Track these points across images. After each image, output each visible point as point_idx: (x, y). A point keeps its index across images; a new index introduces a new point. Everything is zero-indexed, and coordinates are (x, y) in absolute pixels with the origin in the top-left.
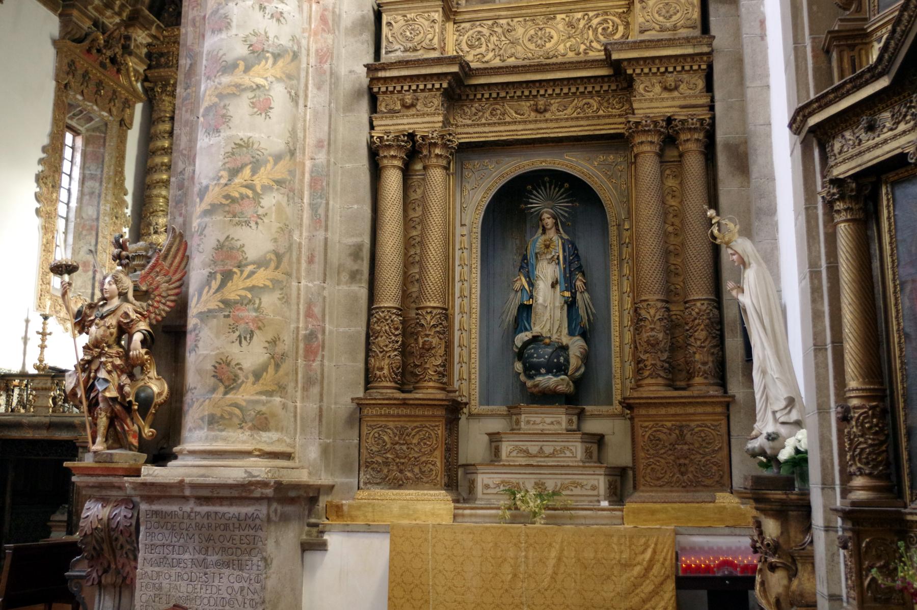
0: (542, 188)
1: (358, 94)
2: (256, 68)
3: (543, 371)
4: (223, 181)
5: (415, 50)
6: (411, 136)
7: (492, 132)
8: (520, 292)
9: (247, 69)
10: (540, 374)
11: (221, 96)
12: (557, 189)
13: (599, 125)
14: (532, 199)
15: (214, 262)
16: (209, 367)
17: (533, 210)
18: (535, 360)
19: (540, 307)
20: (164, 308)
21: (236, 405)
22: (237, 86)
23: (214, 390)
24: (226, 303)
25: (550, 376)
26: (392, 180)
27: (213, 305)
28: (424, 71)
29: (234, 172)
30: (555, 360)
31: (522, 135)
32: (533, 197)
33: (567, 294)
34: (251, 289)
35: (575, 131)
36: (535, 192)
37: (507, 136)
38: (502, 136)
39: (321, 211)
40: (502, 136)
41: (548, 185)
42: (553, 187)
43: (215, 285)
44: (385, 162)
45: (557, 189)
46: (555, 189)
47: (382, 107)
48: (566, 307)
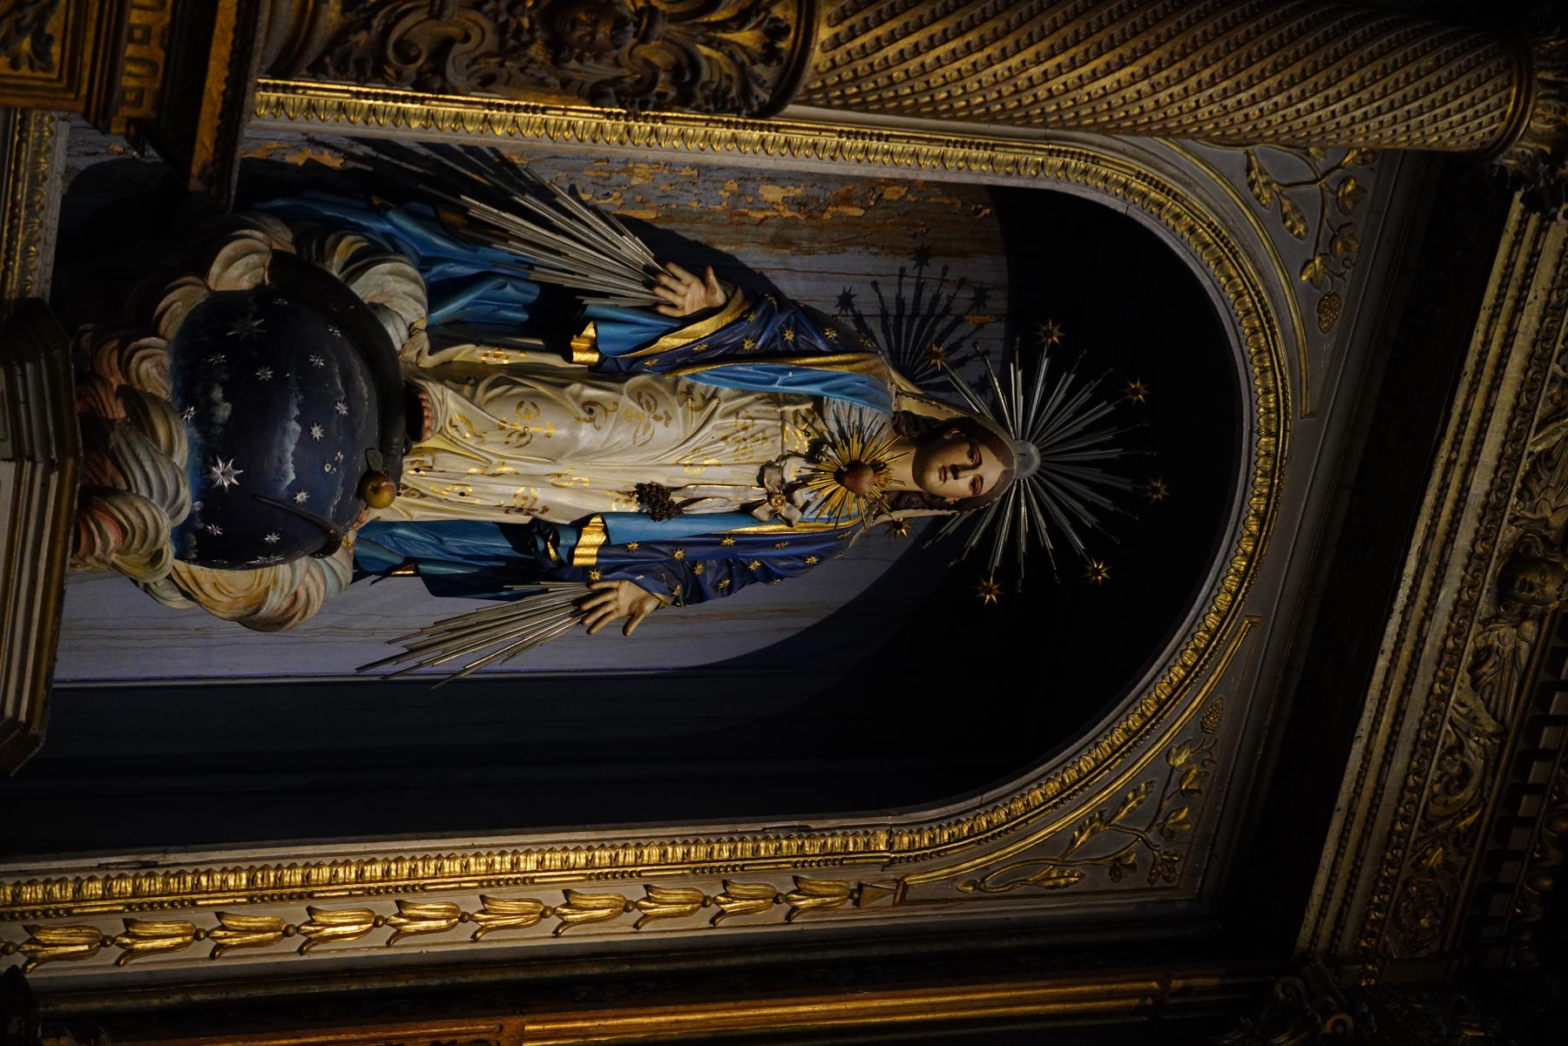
0: (1114, 453)
3: (224, 475)
7: (1507, 346)
8: (644, 296)
10: (205, 456)
12: (1089, 520)
13: (1366, 833)
14: (1071, 393)
17: (1016, 377)
18: (295, 427)
19: (562, 433)
25: (188, 500)
30: (272, 538)
31: (1444, 487)
32: (1085, 396)
33: (592, 538)
35: (1374, 730)
36: (1105, 409)
37: (1465, 413)
38: (1472, 391)
40: (1472, 391)
41: (1125, 484)
42: (1106, 503)
45: (1089, 520)
46: (1093, 508)
48: (524, 519)
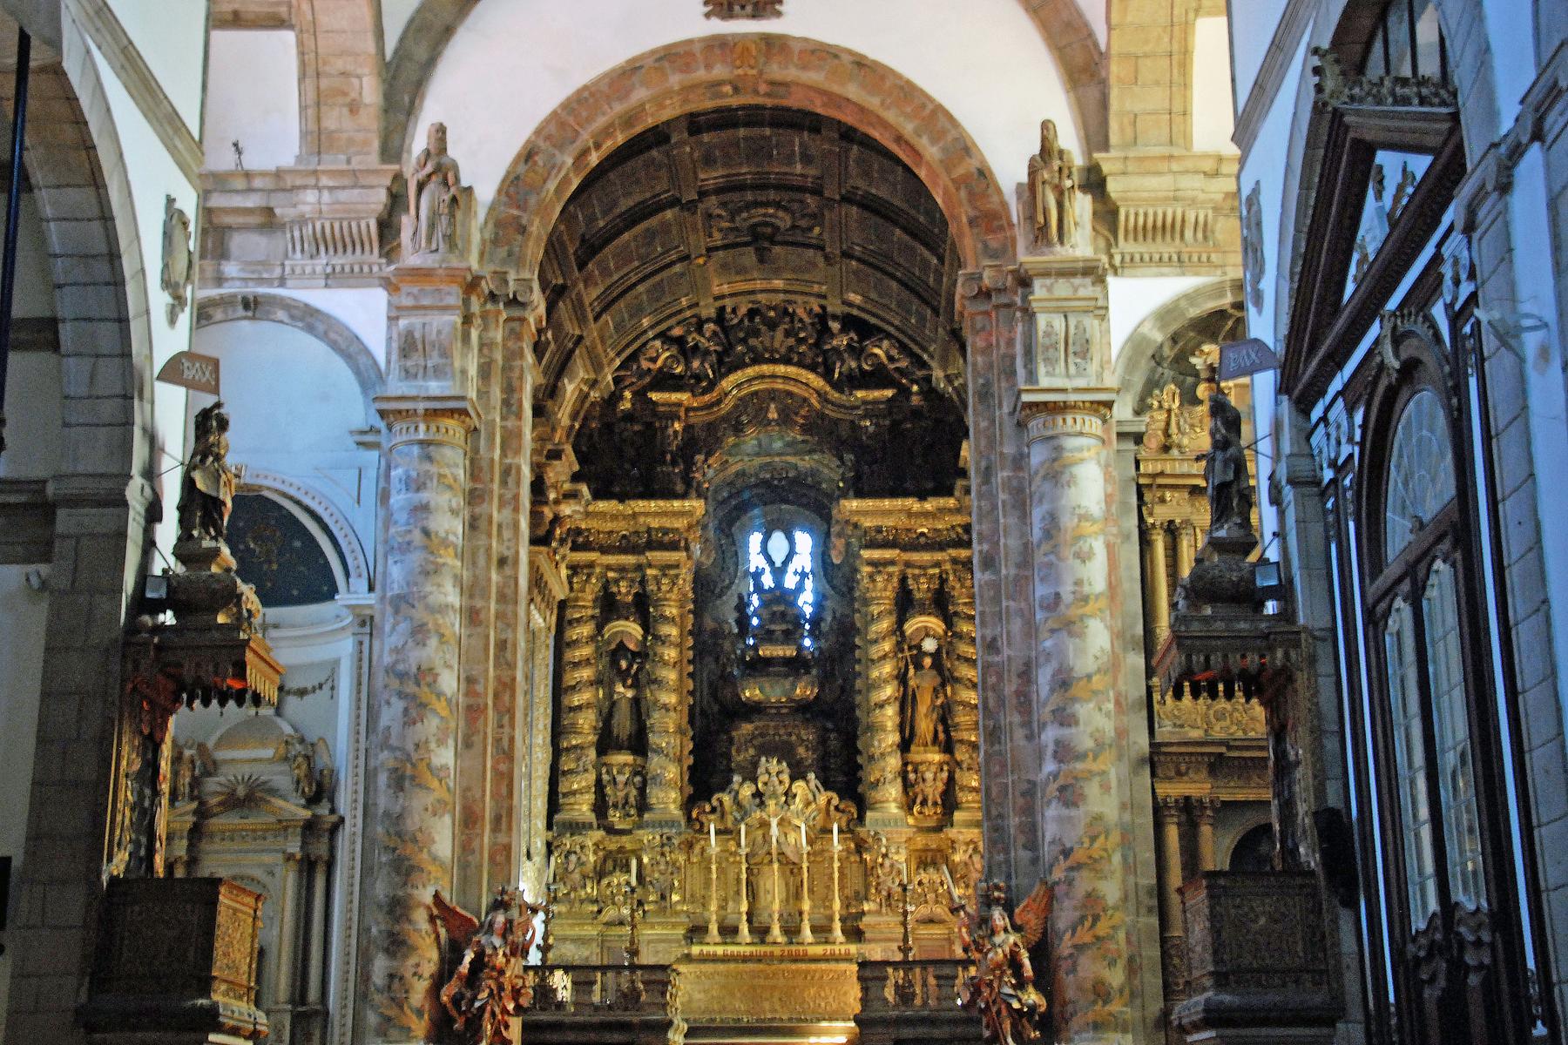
1: (1142, 761)
2: (1101, 758)
4: (1086, 845)
5: (1182, 726)
6: (1187, 798)
9: (1095, 758)
11: (1076, 778)
15: (1084, 906)
16: (1089, 985)
20: (1034, 939)
21: (1110, 1014)
22: (1090, 772)
23: (1095, 1002)
24: (1098, 938)
26: (1172, 834)
27: (1087, 939)
28: (1199, 750)
29: (1093, 839)
34: (1113, 927)
39: (1131, 860)
43: (1087, 924)
44: (1169, 820)
47: (1159, 772)
